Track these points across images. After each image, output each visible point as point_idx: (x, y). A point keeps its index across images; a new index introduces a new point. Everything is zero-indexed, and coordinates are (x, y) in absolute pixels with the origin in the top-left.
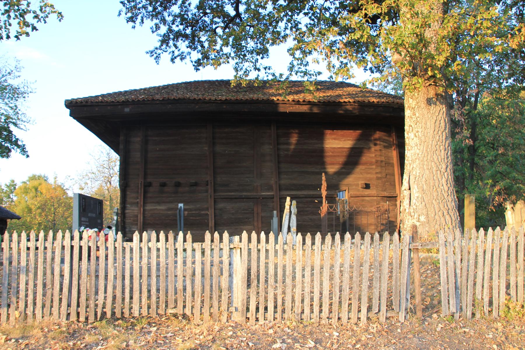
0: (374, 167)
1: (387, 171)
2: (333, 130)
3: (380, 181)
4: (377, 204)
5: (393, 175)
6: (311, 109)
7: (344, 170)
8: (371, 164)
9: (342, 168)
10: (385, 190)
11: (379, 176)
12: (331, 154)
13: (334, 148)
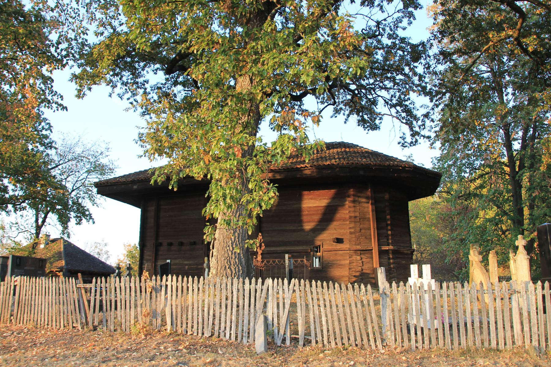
0: (348, 222)
1: (361, 226)
2: (310, 191)
3: (353, 236)
4: (350, 258)
5: (370, 229)
7: (319, 227)
8: (345, 220)
9: (317, 225)
11: (352, 230)
12: (307, 213)
13: (310, 207)
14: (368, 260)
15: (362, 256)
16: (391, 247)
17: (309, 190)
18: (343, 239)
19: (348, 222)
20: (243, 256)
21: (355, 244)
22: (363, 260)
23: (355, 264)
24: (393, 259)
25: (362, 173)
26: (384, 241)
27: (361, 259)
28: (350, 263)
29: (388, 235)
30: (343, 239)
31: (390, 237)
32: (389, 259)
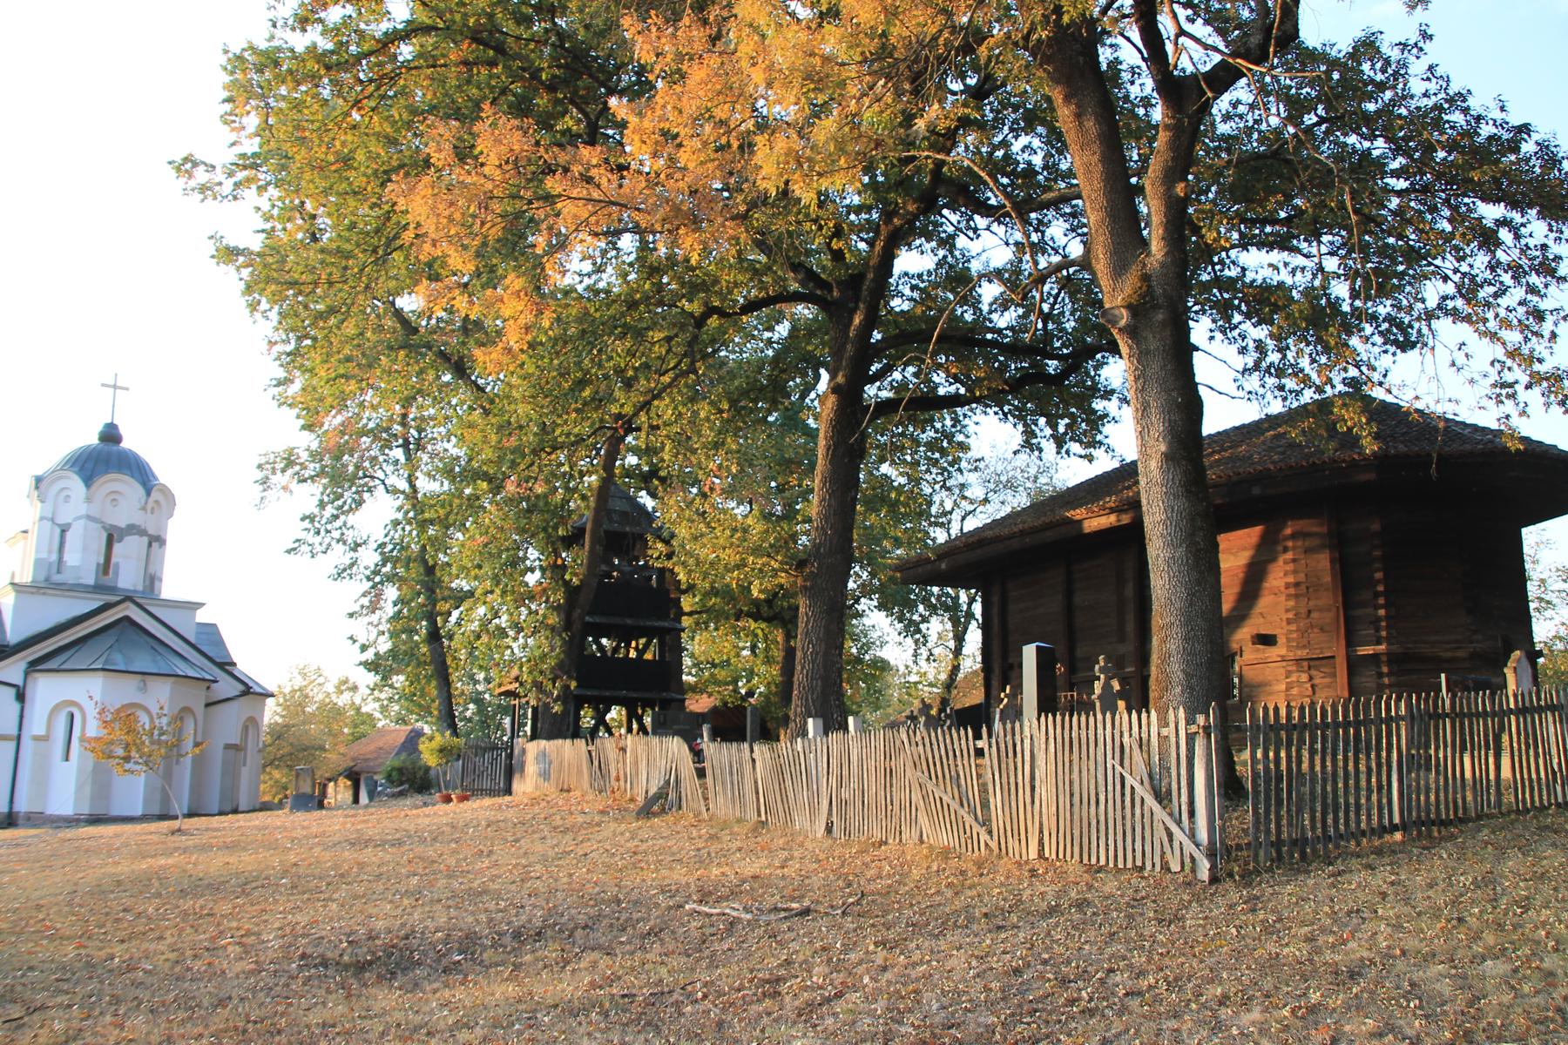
1: (1311, 603)
3: (1293, 627)
6: (1119, 521)
10: (1304, 647)
11: (1290, 615)
14: (1327, 680)
15: (1313, 672)
16: (1382, 647)
18: (1275, 636)
21: (1297, 647)
22: (1316, 681)
23: (1295, 691)
24: (1389, 675)
25: (1256, 491)
27: (1311, 678)
28: (1287, 690)
29: (1379, 619)
30: (1275, 636)
31: (1383, 624)
32: (1380, 675)
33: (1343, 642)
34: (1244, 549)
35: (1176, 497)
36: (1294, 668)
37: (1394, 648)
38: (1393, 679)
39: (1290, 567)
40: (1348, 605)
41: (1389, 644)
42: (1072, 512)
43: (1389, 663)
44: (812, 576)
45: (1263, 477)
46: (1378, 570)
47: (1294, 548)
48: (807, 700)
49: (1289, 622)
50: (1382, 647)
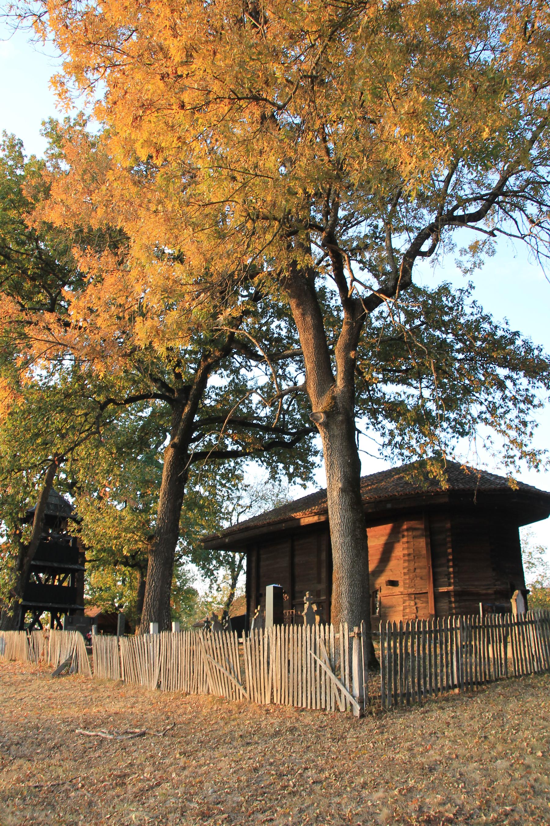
1: (416, 565)
3: (407, 577)
11: (406, 571)
14: (424, 605)
15: (417, 601)
16: (451, 588)
17: (370, 527)
19: (402, 561)
20: (154, 613)
21: (409, 587)
22: (419, 605)
23: (407, 611)
24: (455, 602)
25: (389, 506)
26: (444, 581)
27: (416, 604)
28: (404, 610)
29: (449, 573)
31: (452, 576)
33: (432, 585)
34: (383, 535)
35: (346, 511)
36: (407, 598)
37: (457, 588)
38: (457, 604)
39: (406, 545)
40: (434, 566)
41: (455, 586)
42: (295, 514)
43: (455, 596)
44: (156, 544)
45: (392, 499)
46: (449, 548)
47: (408, 536)
48: (150, 612)
49: (405, 574)
50: (451, 588)
